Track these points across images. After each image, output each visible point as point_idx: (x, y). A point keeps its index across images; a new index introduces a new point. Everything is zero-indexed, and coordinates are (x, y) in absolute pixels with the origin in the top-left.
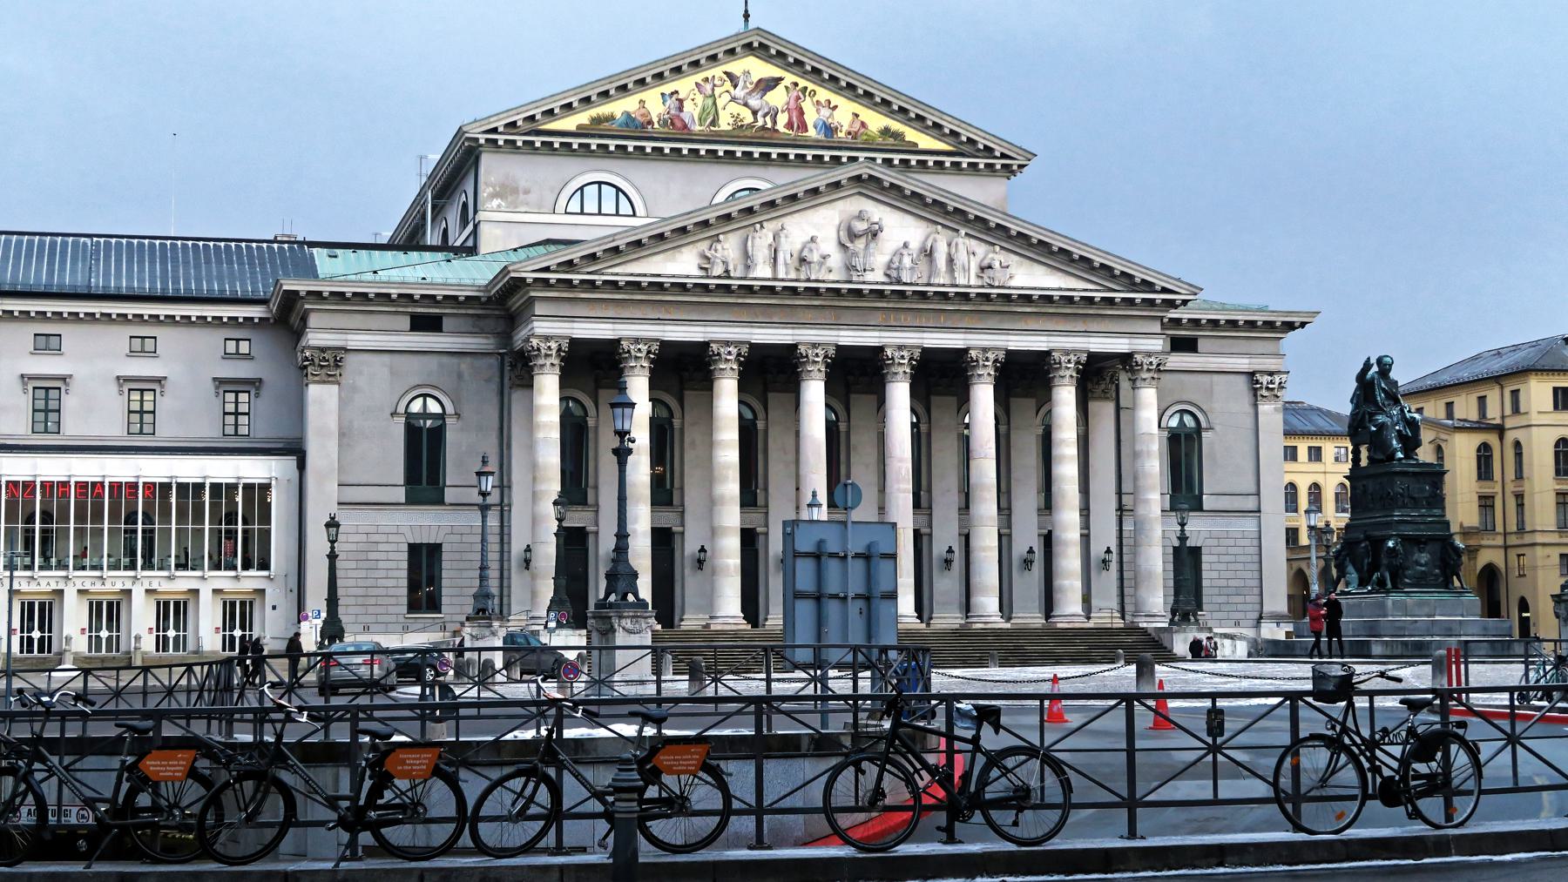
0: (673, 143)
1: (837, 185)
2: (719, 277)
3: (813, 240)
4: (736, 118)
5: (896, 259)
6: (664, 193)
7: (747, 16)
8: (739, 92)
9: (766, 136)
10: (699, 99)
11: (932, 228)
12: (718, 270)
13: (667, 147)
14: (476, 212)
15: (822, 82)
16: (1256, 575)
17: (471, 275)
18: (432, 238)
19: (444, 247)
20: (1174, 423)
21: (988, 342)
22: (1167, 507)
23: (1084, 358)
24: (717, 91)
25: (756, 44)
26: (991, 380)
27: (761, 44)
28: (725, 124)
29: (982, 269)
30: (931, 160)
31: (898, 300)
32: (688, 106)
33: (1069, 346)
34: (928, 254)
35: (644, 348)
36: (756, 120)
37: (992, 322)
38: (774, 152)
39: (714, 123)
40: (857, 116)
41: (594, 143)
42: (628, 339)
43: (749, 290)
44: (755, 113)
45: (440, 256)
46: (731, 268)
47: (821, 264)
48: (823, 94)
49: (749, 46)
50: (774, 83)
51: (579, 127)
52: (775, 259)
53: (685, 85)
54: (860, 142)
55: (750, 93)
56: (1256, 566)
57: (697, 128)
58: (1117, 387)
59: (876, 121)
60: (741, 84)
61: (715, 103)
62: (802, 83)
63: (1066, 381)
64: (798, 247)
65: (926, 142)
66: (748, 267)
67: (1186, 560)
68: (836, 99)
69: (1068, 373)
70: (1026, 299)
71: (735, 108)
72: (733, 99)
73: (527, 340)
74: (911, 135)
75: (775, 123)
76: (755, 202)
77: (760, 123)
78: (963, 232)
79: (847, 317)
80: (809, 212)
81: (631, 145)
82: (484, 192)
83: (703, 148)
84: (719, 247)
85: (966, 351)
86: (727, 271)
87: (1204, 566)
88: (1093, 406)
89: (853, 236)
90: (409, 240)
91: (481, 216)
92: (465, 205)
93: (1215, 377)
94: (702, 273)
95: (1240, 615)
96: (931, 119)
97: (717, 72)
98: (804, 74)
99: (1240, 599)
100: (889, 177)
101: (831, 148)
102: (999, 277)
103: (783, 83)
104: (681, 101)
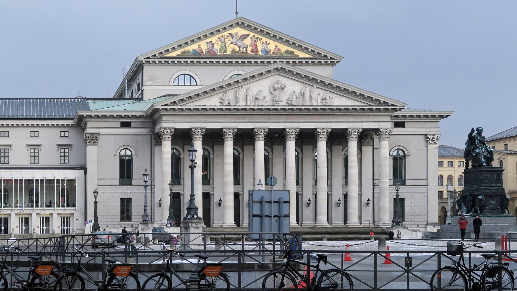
0: (210, 59)
1: (269, 71)
2: (227, 106)
3: (260, 91)
4: (233, 49)
5: (291, 97)
6: (208, 76)
7: (237, 13)
8: (234, 40)
9: (244, 55)
10: (220, 43)
11: (304, 85)
12: (226, 103)
13: (208, 61)
14: (142, 86)
15: (264, 35)
16: (426, 208)
17: (140, 108)
18: (128, 95)
19: (132, 98)
20: (395, 153)
21: (324, 126)
22: (392, 184)
23: (361, 131)
24: (226, 40)
25: (240, 23)
26: (326, 139)
27: (242, 23)
28: (229, 51)
29: (323, 100)
30: (304, 61)
31: (291, 111)
32: (216, 46)
33: (355, 126)
34: (303, 95)
35: (200, 131)
36: (240, 50)
37: (326, 119)
38: (246, 61)
39: (225, 51)
40: (277, 46)
41: (183, 61)
42: (194, 128)
43: (237, 109)
44: (239, 47)
45: (130, 101)
46: (231, 102)
47: (263, 100)
48: (264, 39)
49: (238, 23)
50: (246, 36)
51: (178, 55)
52: (246, 99)
53: (214, 39)
54: (278, 56)
55: (238, 40)
56: (426, 205)
58: (373, 141)
59: (284, 48)
61: (225, 45)
62: (257, 36)
63: (354, 139)
64: (255, 94)
65: (302, 55)
66: (237, 102)
67: (399, 204)
68: (269, 41)
69: (354, 136)
70: (339, 110)
71: (232, 46)
72: (232, 43)
73: (160, 129)
74: (297, 52)
75: (247, 50)
76: (239, 78)
77: (241, 51)
78: (315, 87)
79: (273, 118)
80: (259, 81)
81: (195, 61)
82: (144, 80)
83: (221, 61)
84: (226, 95)
85: (316, 129)
86: (229, 103)
87: (405, 205)
88: (364, 148)
89: (275, 89)
90: (120, 97)
91: (144, 87)
92: (139, 84)
94: (221, 104)
95: (419, 223)
96: (304, 46)
97: (226, 33)
98: (257, 33)
99: (420, 217)
100: (288, 68)
101: (267, 59)
102: (329, 102)
103: (250, 36)
104: (213, 44)
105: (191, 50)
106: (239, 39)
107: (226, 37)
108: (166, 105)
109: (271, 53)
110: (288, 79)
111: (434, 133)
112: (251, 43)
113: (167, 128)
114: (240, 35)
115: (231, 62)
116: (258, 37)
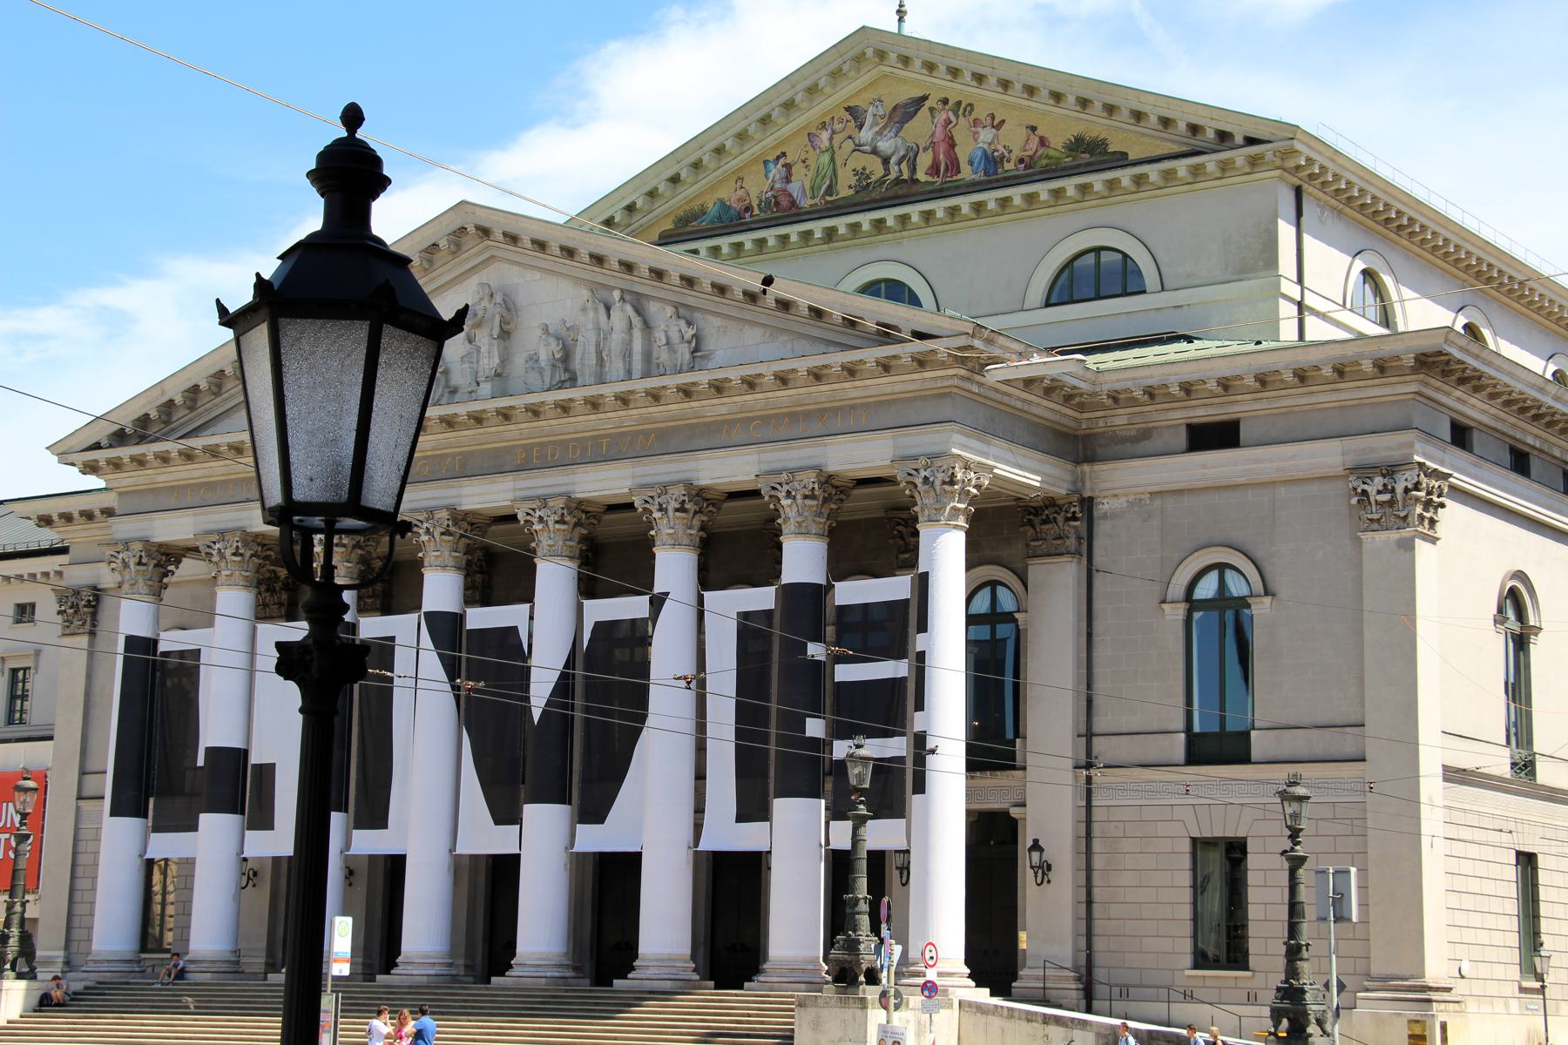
4: (861, 174)
7: (901, 13)
8: (866, 135)
20: (1207, 589)
24: (837, 139)
32: (798, 171)
36: (887, 171)
39: (830, 190)
40: (1033, 129)
44: (886, 161)
55: (879, 133)
57: (806, 203)
60: (869, 120)
61: (832, 160)
71: (858, 161)
72: (858, 148)
75: (913, 170)
77: (893, 176)
93: (1282, 491)
103: (928, 104)
104: (788, 166)
105: (711, 205)
106: (884, 127)
107: (838, 127)
108: (97, 446)
109: (1008, 166)
110: (537, 275)
111: (1396, 455)
112: (933, 135)
113: (127, 544)
114: (890, 103)
115: (830, 234)
116: (959, 103)
